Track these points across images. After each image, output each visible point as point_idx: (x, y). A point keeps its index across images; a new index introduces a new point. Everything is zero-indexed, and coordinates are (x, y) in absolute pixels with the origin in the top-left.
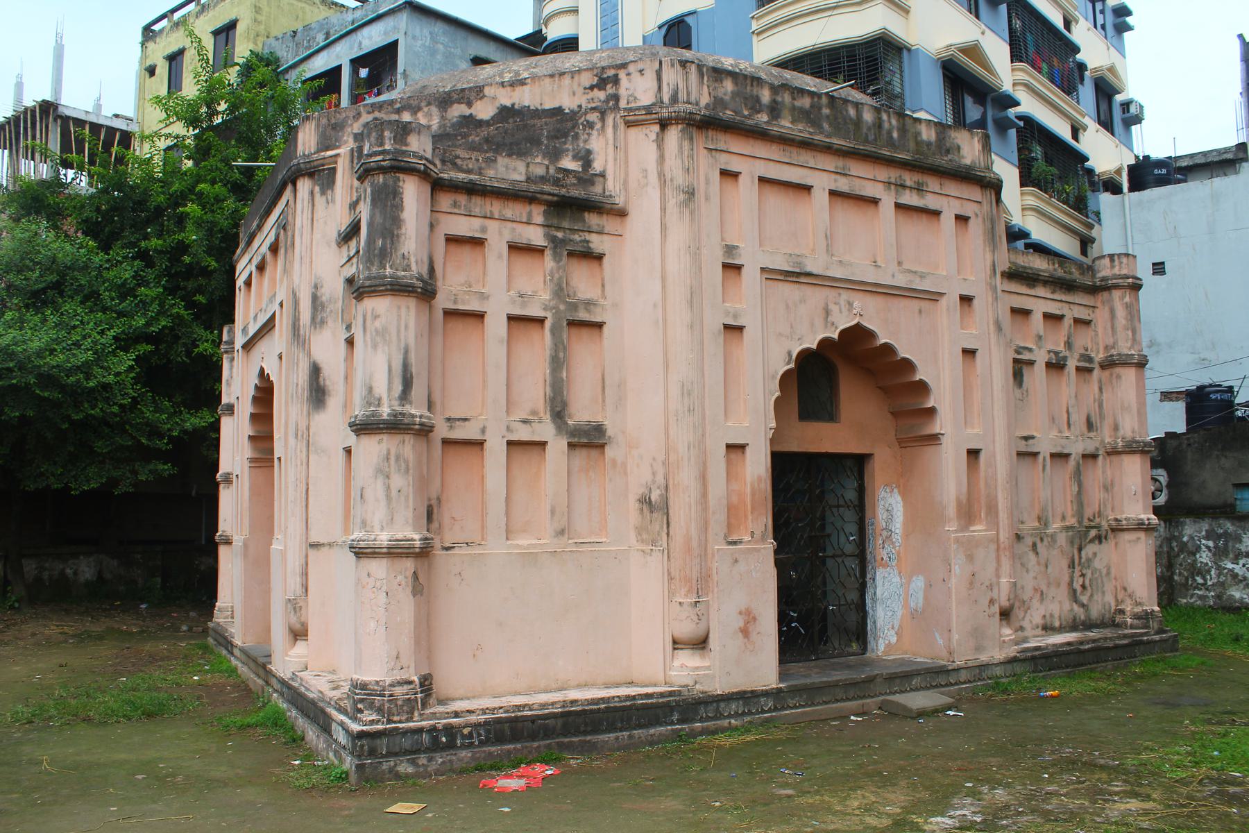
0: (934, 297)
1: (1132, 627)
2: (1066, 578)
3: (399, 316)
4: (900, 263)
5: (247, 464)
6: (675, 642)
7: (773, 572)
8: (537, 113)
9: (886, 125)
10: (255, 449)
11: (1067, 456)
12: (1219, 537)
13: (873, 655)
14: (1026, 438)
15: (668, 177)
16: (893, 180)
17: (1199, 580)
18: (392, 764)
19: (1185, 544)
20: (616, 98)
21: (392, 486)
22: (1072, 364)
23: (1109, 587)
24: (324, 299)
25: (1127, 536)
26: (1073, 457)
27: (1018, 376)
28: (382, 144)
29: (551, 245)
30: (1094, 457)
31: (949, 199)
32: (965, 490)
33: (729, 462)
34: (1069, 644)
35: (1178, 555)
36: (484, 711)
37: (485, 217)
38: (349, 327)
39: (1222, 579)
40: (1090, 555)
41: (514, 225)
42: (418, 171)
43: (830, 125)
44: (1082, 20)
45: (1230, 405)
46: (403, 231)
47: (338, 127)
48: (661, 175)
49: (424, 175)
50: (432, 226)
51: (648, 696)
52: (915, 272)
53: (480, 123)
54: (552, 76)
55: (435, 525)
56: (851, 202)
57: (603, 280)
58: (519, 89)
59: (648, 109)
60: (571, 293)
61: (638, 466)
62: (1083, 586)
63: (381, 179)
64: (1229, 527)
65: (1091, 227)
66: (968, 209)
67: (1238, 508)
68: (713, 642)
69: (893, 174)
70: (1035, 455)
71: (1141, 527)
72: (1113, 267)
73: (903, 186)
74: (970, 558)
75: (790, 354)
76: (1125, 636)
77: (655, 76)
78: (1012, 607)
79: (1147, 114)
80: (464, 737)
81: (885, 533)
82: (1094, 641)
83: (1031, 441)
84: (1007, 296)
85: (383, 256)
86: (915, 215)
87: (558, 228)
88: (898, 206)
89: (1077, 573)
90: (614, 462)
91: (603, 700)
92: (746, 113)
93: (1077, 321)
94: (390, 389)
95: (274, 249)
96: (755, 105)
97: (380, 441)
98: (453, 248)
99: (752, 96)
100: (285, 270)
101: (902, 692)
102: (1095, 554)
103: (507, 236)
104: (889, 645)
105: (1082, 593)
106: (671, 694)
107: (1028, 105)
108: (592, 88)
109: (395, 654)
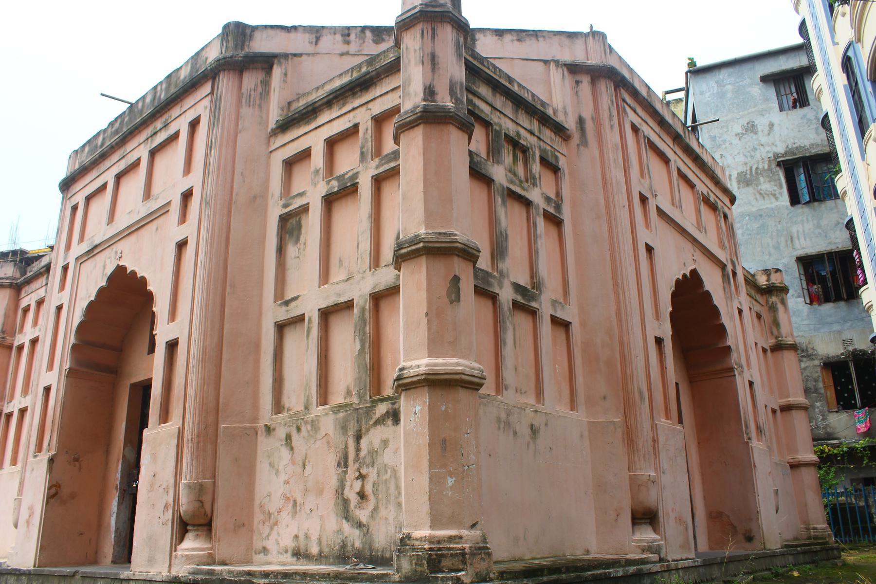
2: (334, 482)
11: (348, 305)
40: (376, 443)
62: (362, 495)
83: (293, 304)
89: (352, 473)
102: (385, 443)
105: (359, 506)
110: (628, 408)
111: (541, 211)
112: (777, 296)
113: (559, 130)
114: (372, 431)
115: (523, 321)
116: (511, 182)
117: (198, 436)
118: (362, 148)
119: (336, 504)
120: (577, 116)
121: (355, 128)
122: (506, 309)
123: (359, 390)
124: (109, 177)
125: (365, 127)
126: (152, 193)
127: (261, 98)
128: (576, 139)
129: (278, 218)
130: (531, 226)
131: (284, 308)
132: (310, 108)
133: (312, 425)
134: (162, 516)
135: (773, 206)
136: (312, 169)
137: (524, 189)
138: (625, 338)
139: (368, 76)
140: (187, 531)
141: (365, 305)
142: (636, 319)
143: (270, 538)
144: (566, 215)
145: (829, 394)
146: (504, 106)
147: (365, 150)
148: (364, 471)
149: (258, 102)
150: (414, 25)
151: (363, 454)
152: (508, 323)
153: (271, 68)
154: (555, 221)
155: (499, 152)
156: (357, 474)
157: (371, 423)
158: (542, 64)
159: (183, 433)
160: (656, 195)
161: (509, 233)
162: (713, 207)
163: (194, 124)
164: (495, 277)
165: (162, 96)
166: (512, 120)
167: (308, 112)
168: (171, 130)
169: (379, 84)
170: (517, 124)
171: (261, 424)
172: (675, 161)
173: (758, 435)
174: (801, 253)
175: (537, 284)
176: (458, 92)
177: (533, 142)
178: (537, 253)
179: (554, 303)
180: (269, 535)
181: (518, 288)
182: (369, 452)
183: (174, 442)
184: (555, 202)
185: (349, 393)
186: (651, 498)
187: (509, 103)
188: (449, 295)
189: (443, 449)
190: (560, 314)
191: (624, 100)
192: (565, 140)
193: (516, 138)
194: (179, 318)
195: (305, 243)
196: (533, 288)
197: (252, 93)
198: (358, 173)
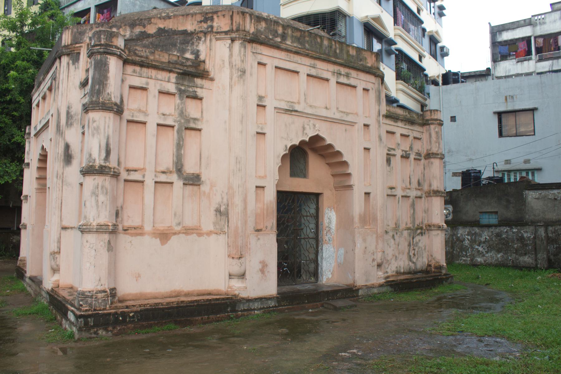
0: (352, 124)
1: (434, 272)
2: (407, 251)
3: (105, 121)
4: (337, 108)
5: (34, 191)
6: (230, 275)
7: (275, 245)
8: (176, 32)
9: (334, 47)
10: (39, 184)
11: (409, 197)
12: (473, 234)
13: (321, 283)
14: (392, 188)
15: (234, 64)
16: (336, 71)
17: (464, 253)
18: (95, 330)
19: (459, 237)
20: (212, 27)
21: (99, 201)
22: (412, 156)
23: (425, 255)
24: (72, 113)
25: (434, 233)
26: (411, 197)
27: (388, 161)
28: (100, 41)
29: (179, 92)
30: (420, 197)
31: (361, 80)
32: (363, 210)
33: (257, 194)
34: (407, 279)
35: (456, 242)
36: (140, 306)
37: (148, 78)
38: (83, 127)
39: (473, 252)
41: (162, 82)
42: (117, 55)
43: (309, 45)
44: (425, 10)
45: (479, 178)
46: (109, 82)
47: (82, 33)
48: (230, 63)
49: (120, 57)
50: (123, 81)
51: (217, 299)
52: (345, 112)
53: (149, 36)
54: (183, 16)
55: (120, 219)
56: (316, 79)
57: (202, 109)
58: (168, 21)
59: (226, 33)
60: (187, 115)
61: (215, 195)
62: (414, 254)
63: (99, 57)
64: (477, 230)
65: (426, 100)
66: (369, 86)
67: (481, 223)
68: (247, 276)
69: (336, 68)
70: (395, 196)
71: (439, 227)
72: (431, 115)
73: (340, 74)
74: (364, 240)
75: (286, 146)
76: (431, 276)
77: (230, 18)
78: (382, 263)
79: (450, 53)
80: (130, 317)
81: (327, 229)
82: (418, 278)
83: (393, 190)
84: (385, 126)
85: (99, 93)
86: (345, 87)
87: (182, 85)
88: (338, 83)
90: (204, 193)
91: (196, 301)
92: (271, 37)
93: (415, 138)
94: (99, 155)
95: (50, 89)
96: (276, 34)
97: (94, 179)
98: (133, 91)
99: (274, 30)
100: (54, 99)
101: (332, 299)
102: (420, 240)
103: (158, 87)
104: (328, 279)
105: (413, 257)
106: (228, 299)
107: (401, 45)
108: (201, 22)
109: (98, 279)
121: (408, 136)
131: (390, 190)
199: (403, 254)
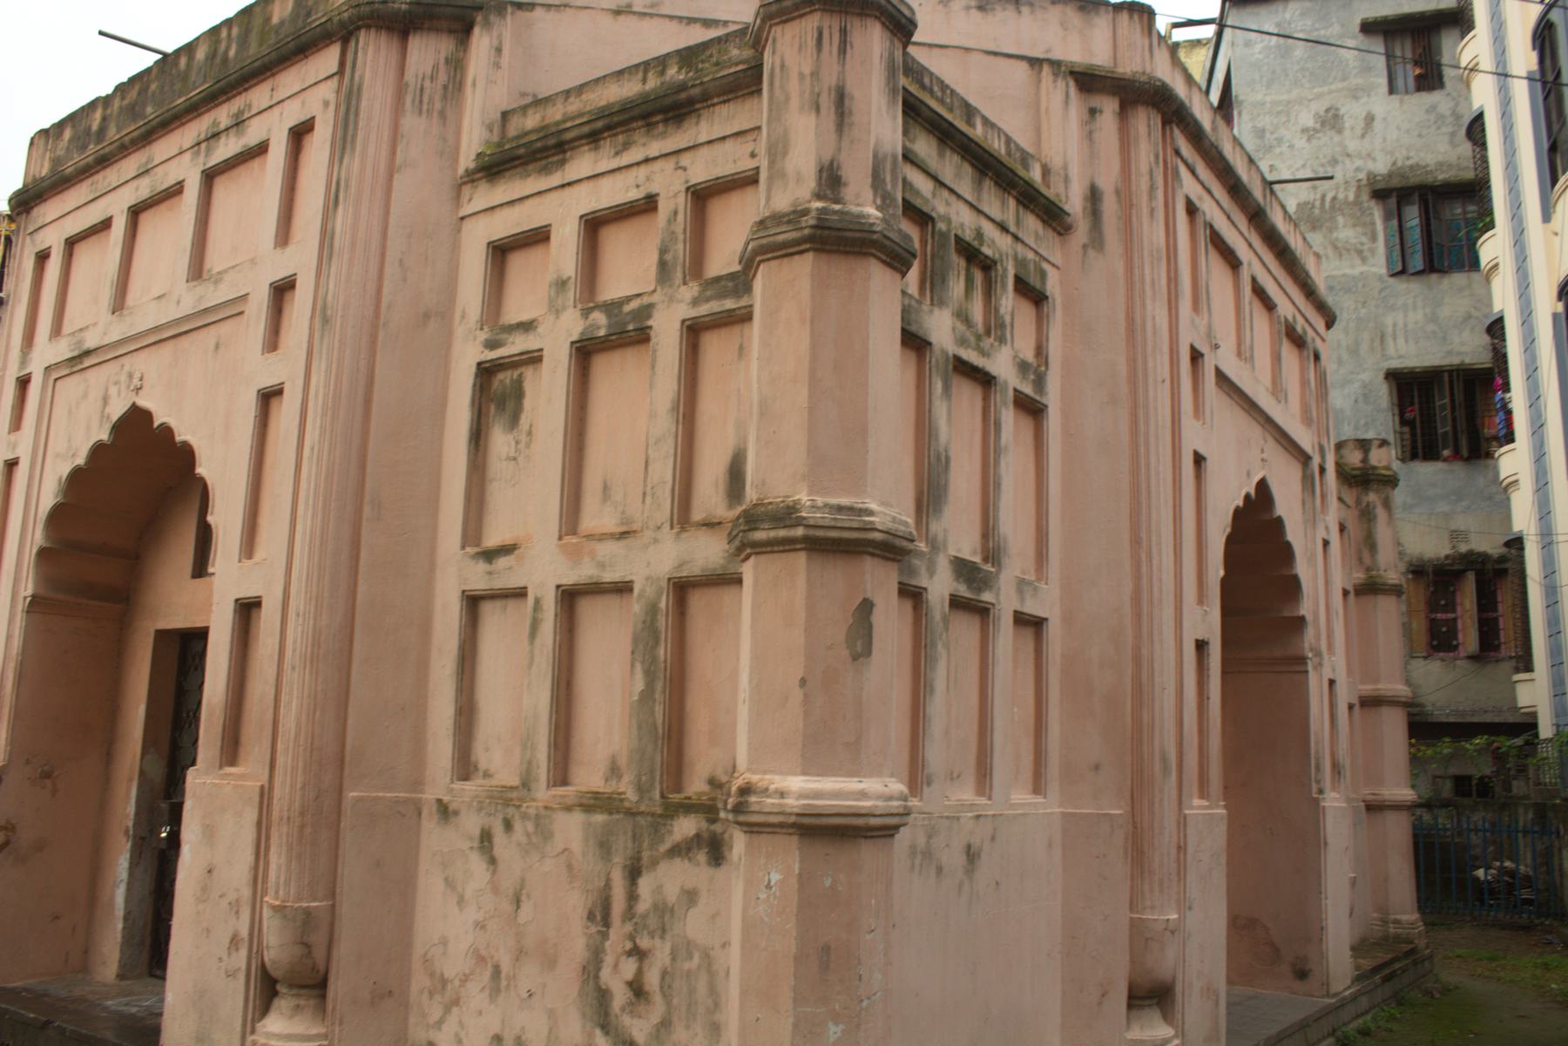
2: (577, 946)
11: (623, 588)
40: (672, 893)
62: (637, 989)
70: (521, 593)
83: (502, 562)
102: (691, 896)
105: (631, 1008)
110: (1139, 791)
111: (1011, 394)
112: (1377, 491)
113: (1053, 216)
114: (663, 867)
115: (965, 630)
116: (962, 342)
117: (302, 814)
118: (663, 251)
119: (581, 993)
120: (1087, 183)
122: (937, 616)
123: (639, 777)
124: (117, 206)
125: (672, 207)
126: (207, 266)
127: (445, 97)
128: (1081, 233)
129: (474, 369)
130: (990, 426)
131: (482, 566)
132: (552, 141)
133: (537, 826)
134: (225, 957)
135: (1356, 272)
136: (550, 276)
137: (984, 353)
138: (1145, 651)
139: (683, 95)
140: (275, 994)
141: (659, 598)
142: (1168, 613)
143: (445, 1027)
144: (1053, 398)
145: (1415, 625)
146: (958, 175)
147: (668, 257)
148: (644, 942)
149: (438, 106)
150: (801, 16)
151: (643, 906)
152: (940, 647)
153: (467, 30)
154: (1031, 408)
155: (944, 280)
156: (629, 945)
157: (664, 847)
158: (1024, 65)
159: (270, 799)
160: (1217, 347)
161: (952, 454)
162: (1298, 341)
163: (300, 134)
164: (920, 554)
165: (232, 53)
166: (972, 206)
167: (546, 148)
168: (252, 137)
169: (705, 113)
170: (979, 212)
171: (430, 795)
172: (1250, 264)
173: (1333, 779)
174: (1395, 364)
175: (993, 551)
176: (888, 179)
177: (1004, 248)
178: (998, 485)
179: (1021, 584)
180: (440, 1022)
181: (963, 569)
182: (655, 906)
183: (251, 815)
184: (1035, 372)
185: (614, 771)
186: (1164, 962)
187: (967, 169)
188: (850, 640)
189: (826, 965)
190: (1032, 608)
191: (1177, 153)
192: (1060, 234)
193: (975, 244)
194: (260, 553)
195: (530, 433)
196: (986, 560)
197: (427, 84)
198: (651, 306)
199: (550, 962)
